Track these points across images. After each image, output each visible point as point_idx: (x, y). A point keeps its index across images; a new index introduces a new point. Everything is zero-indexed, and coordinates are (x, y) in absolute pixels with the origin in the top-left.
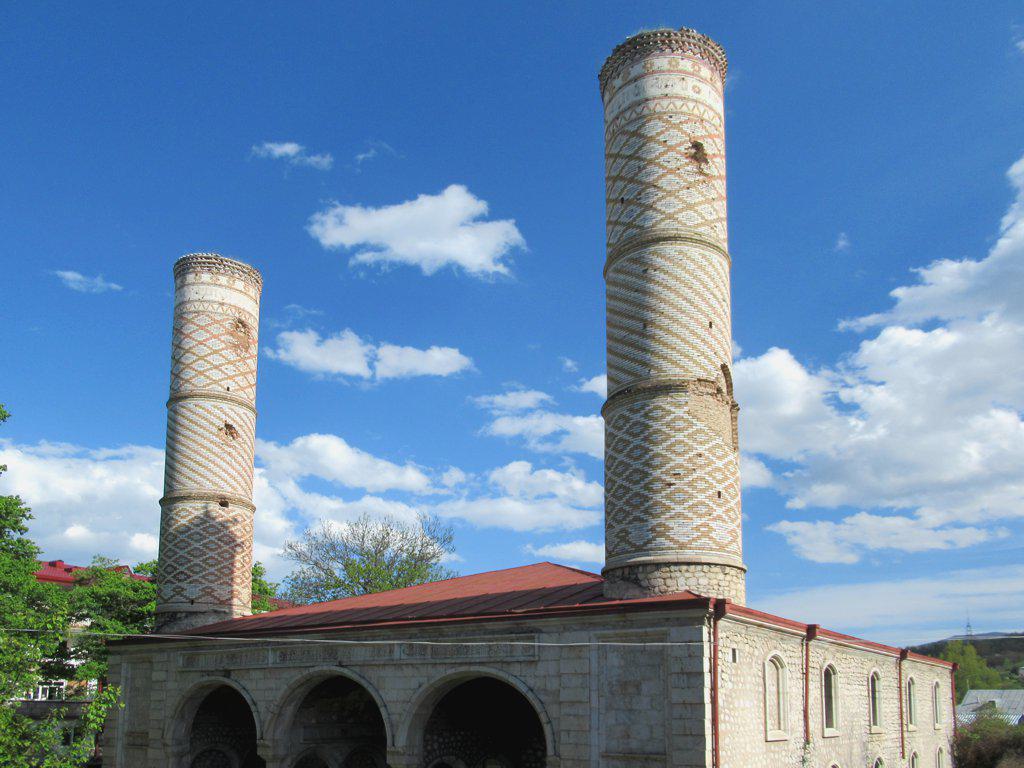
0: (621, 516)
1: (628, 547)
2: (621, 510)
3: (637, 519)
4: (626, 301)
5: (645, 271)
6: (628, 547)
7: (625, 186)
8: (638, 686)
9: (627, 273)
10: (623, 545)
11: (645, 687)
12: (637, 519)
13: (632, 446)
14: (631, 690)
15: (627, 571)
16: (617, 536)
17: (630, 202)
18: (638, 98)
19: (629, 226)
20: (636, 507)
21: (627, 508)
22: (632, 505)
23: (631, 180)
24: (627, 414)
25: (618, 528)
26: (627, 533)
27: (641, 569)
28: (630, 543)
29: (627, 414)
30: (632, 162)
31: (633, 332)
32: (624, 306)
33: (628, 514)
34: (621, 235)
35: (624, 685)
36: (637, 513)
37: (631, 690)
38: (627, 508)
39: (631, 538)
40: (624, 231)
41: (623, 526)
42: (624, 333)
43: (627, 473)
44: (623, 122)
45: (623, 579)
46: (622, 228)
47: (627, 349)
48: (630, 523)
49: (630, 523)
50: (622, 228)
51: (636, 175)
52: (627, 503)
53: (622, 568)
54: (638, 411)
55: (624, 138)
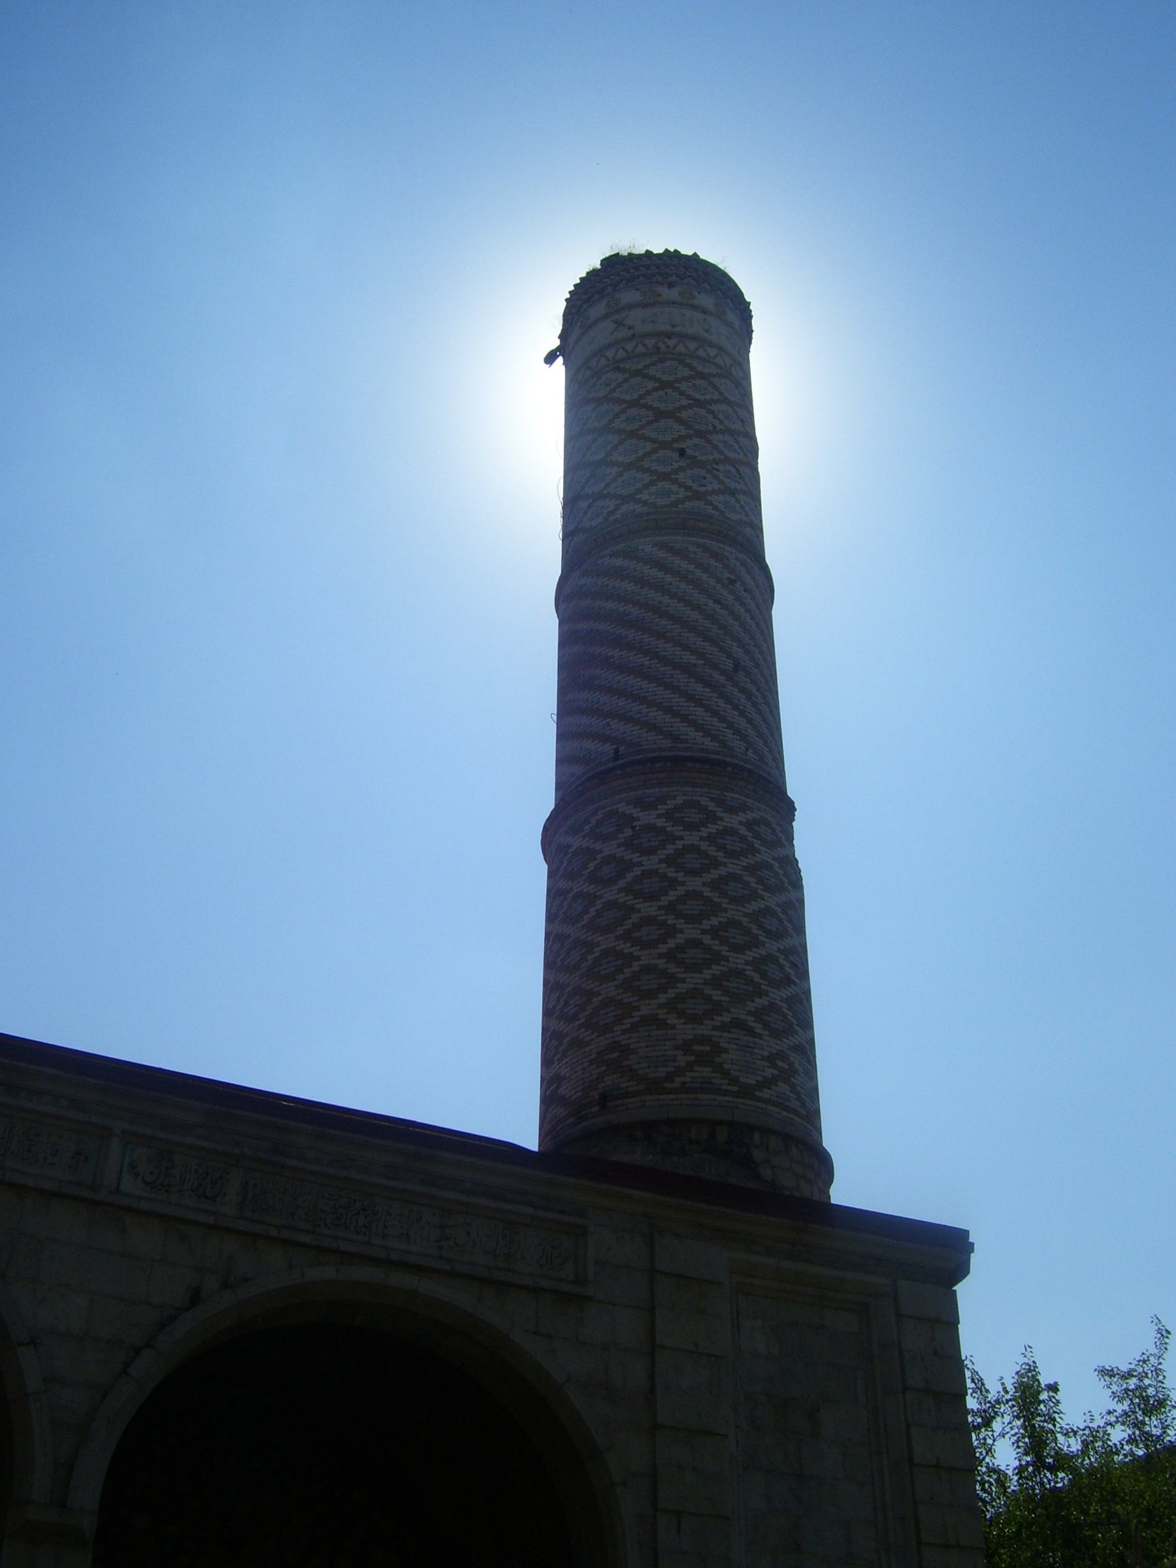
3: (737, 1024)
4: (697, 608)
10: (704, 1072)
13: (723, 871)
19: (697, 496)
21: (717, 995)
24: (711, 806)
29: (711, 806)
31: (715, 667)
38: (717, 995)
42: (693, 659)
43: (715, 921)
46: (682, 493)
47: (699, 689)
48: (724, 1027)
49: (724, 1027)
50: (682, 493)
52: (716, 982)
54: (732, 810)
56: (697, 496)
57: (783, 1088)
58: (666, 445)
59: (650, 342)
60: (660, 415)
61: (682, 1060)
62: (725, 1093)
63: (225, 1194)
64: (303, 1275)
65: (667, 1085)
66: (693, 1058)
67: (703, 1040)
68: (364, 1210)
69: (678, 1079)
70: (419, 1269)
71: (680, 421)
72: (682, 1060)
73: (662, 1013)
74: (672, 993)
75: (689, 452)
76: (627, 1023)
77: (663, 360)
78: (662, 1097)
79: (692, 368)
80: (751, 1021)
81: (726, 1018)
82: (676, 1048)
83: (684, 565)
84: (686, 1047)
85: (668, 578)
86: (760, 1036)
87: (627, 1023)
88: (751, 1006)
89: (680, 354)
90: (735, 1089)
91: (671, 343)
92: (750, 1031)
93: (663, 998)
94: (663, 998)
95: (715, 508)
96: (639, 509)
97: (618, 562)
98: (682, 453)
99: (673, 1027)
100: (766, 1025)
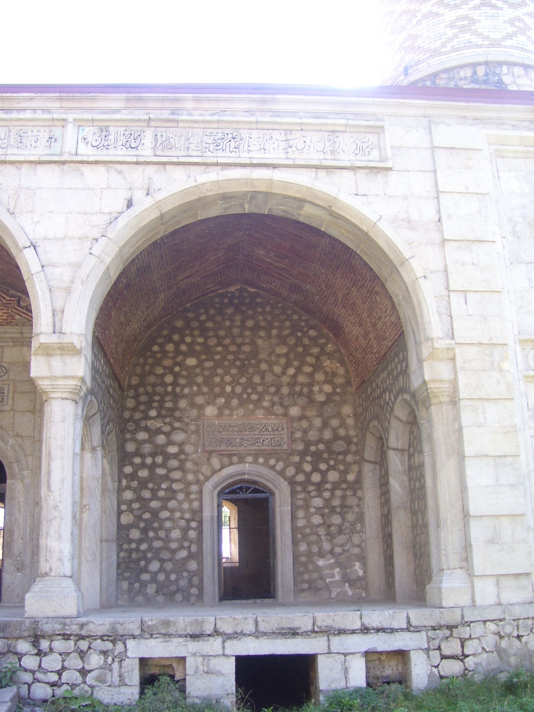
1: (475, 40)
6: (475, 40)
10: (467, 36)
16: (452, 25)
25: (450, 15)
27: (505, 69)
28: (480, 35)
53: (475, 65)
57: (521, 38)
61: (450, 33)
62: (481, 46)
63: (143, 144)
64: (196, 181)
65: (442, 50)
66: (457, 30)
68: (234, 138)
69: (448, 45)
70: (274, 166)
72: (450, 33)
73: (435, 9)
76: (414, 21)
78: (440, 58)
82: (446, 27)
84: (452, 25)
86: (501, 9)
87: (414, 21)
90: (487, 43)
99: (443, 15)
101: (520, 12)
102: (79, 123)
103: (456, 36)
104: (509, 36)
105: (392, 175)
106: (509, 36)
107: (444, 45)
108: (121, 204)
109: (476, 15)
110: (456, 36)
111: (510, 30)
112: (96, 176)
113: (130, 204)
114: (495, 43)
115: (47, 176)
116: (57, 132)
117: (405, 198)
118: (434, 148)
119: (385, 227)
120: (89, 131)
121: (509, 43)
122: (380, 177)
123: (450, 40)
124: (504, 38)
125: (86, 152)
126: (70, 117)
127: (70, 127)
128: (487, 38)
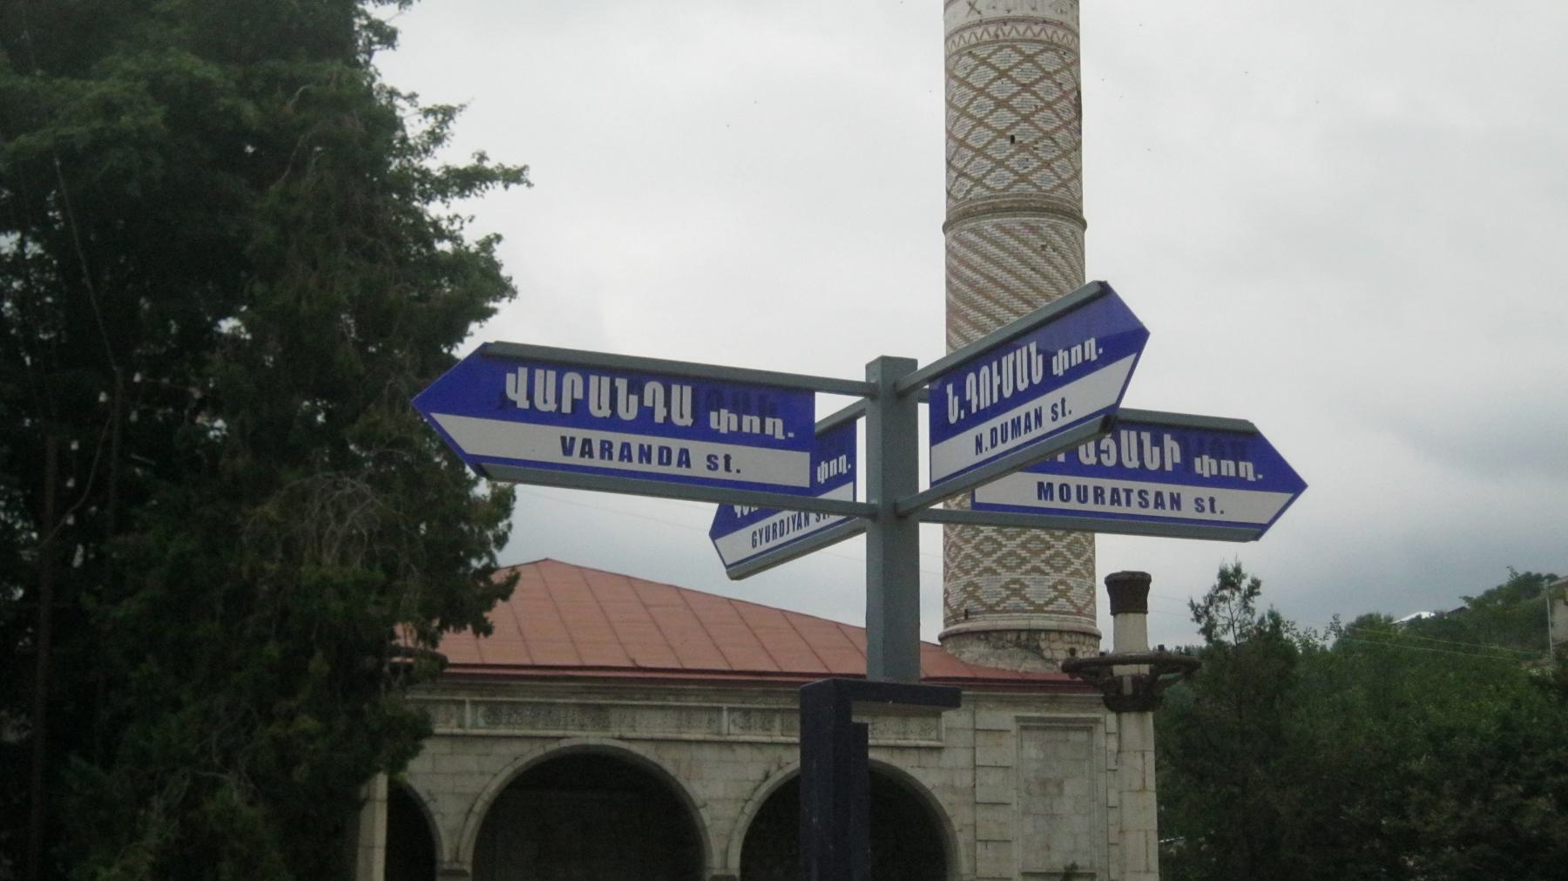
0: (1012, 561)
1: (1024, 605)
2: (1011, 553)
3: (1036, 569)
4: (1019, 277)
5: (1044, 247)
6: (1024, 605)
7: (1017, 123)
8: (1059, 785)
9: (1021, 241)
10: (1015, 600)
11: (1067, 788)
12: (1036, 569)
14: (1052, 789)
15: (1024, 636)
17: (1023, 147)
18: (1032, 13)
19: (1023, 178)
20: (1036, 553)
21: (1024, 553)
22: (1029, 551)
23: (1026, 118)
25: (1006, 576)
26: (1023, 586)
28: (1027, 600)
30: (1027, 95)
32: (1014, 283)
33: (1024, 561)
34: (1010, 186)
35: (1044, 783)
36: (1036, 562)
37: (1052, 789)
38: (1024, 553)
39: (1030, 591)
40: (1015, 182)
41: (1016, 576)
44: (1014, 33)
45: (1018, 644)
46: (1012, 177)
48: (1027, 572)
49: (1027, 572)
50: (1012, 177)
51: (1032, 114)
53: (1019, 631)
55: (1017, 58)
56: (1023, 178)
57: (1062, 601)
58: (1001, 134)
59: (992, 29)
60: (1000, 104)
61: (1004, 593)
67: (1015, 581)
71: (1012, 110)
72: (1004, 593)
74: (999, 554)
75: (1017, 139)
77: (1001, 49)
79: (1021, 53)
80: (1042, 566)
81: (1029, 566)
83: (1013, 242)
85: (1002, 254)
88: (1043, 557)
89: (1014, 40)
91: (1007, 29)
92: (1043, 573)
93: (995, 557)
94: (995, 557)
95: (1035, 185)
96: (986, 193)
97: (972, 237)
98: (1012, 139)
100: (1052, 566)
101: (1062, 576)
102: (731, 710)
103: (1008, 597)
104: (1051, 602)
105: (945, 754)
106: (1051, 602)
107: (998, 604)
108: (761, 776)
109: (1026, 579)
110: (1008, 597)
111: (1053, 594)
112: (743, 753)
113: (767, 776)
114: (1039, 609)
115: (709, 753)
116: (715, 715)
117: (952, 769)
118: (976, 730)
119: (937, 795)
120: (736, 715)
121: (1050, 608)
122: (935, 754)
123: (1003, 600)
124: (1047, 604)
125: (737, 734)
126: (725, 706)
127: (725, 714)
128: (1032, 603)
